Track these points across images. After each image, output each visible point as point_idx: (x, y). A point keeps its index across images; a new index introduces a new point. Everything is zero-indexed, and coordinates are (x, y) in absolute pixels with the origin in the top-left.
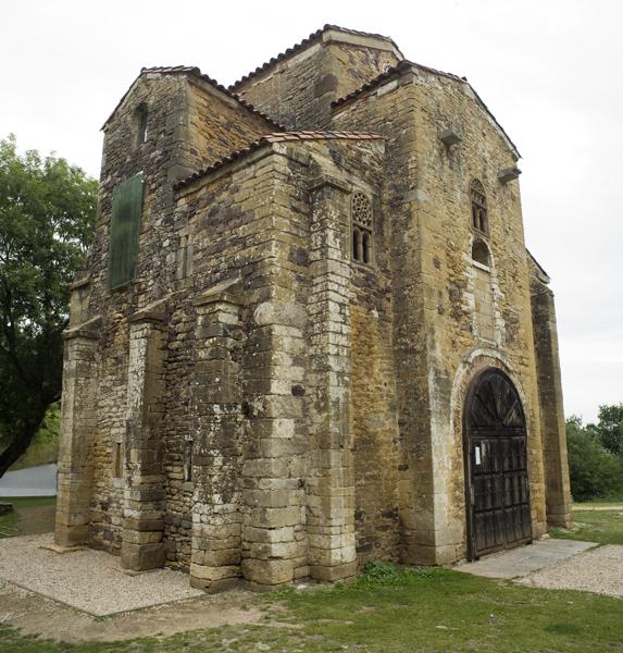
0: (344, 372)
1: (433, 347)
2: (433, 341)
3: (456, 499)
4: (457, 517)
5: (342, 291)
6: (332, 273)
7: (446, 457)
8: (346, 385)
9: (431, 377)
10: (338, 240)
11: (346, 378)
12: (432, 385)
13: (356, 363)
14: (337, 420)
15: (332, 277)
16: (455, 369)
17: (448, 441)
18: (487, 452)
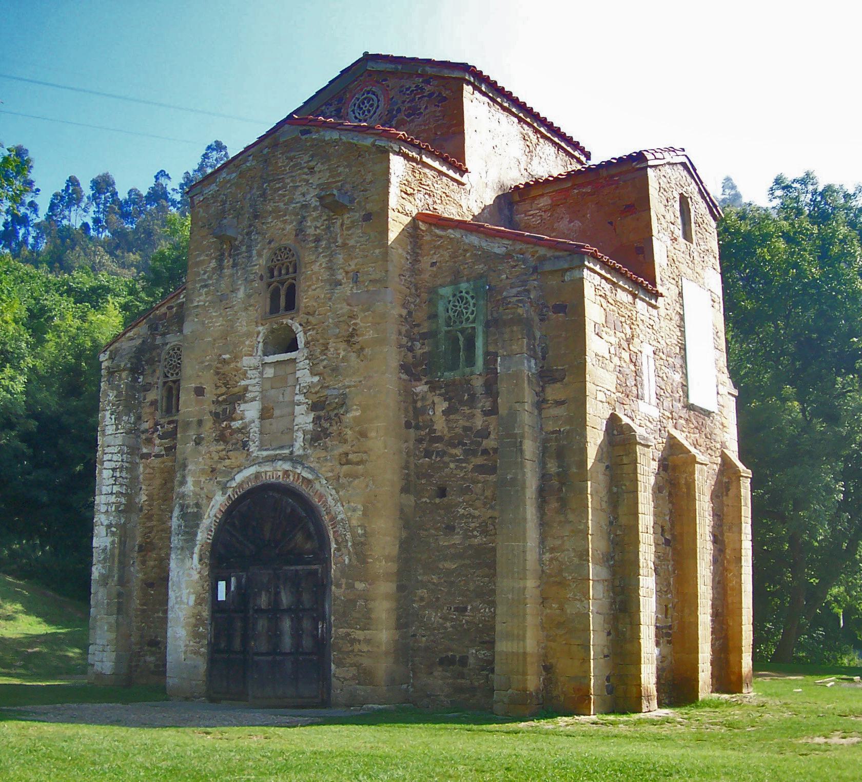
0: (111, 524)
1: (183, 483)
2: (184, 477)
3: (196, 635)
4: (196, 653)
5: (115, 458)
6: (108, 446)
7: (185, 592)
8: (113, 534)
9: (176, 513)
10: (113, 417)
11: (114, 529)
12: (175, 522)
13: (162, 510)
14: (105, 563)
15: (107, 450)
16: (209, 499)
17: (190, 575)
18: (237, 587)
